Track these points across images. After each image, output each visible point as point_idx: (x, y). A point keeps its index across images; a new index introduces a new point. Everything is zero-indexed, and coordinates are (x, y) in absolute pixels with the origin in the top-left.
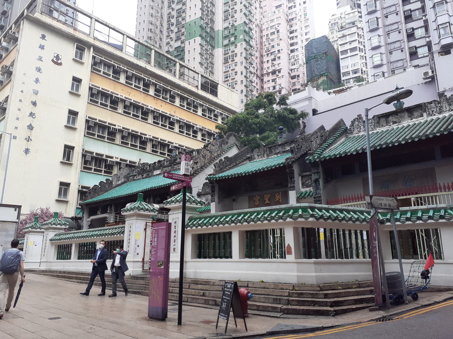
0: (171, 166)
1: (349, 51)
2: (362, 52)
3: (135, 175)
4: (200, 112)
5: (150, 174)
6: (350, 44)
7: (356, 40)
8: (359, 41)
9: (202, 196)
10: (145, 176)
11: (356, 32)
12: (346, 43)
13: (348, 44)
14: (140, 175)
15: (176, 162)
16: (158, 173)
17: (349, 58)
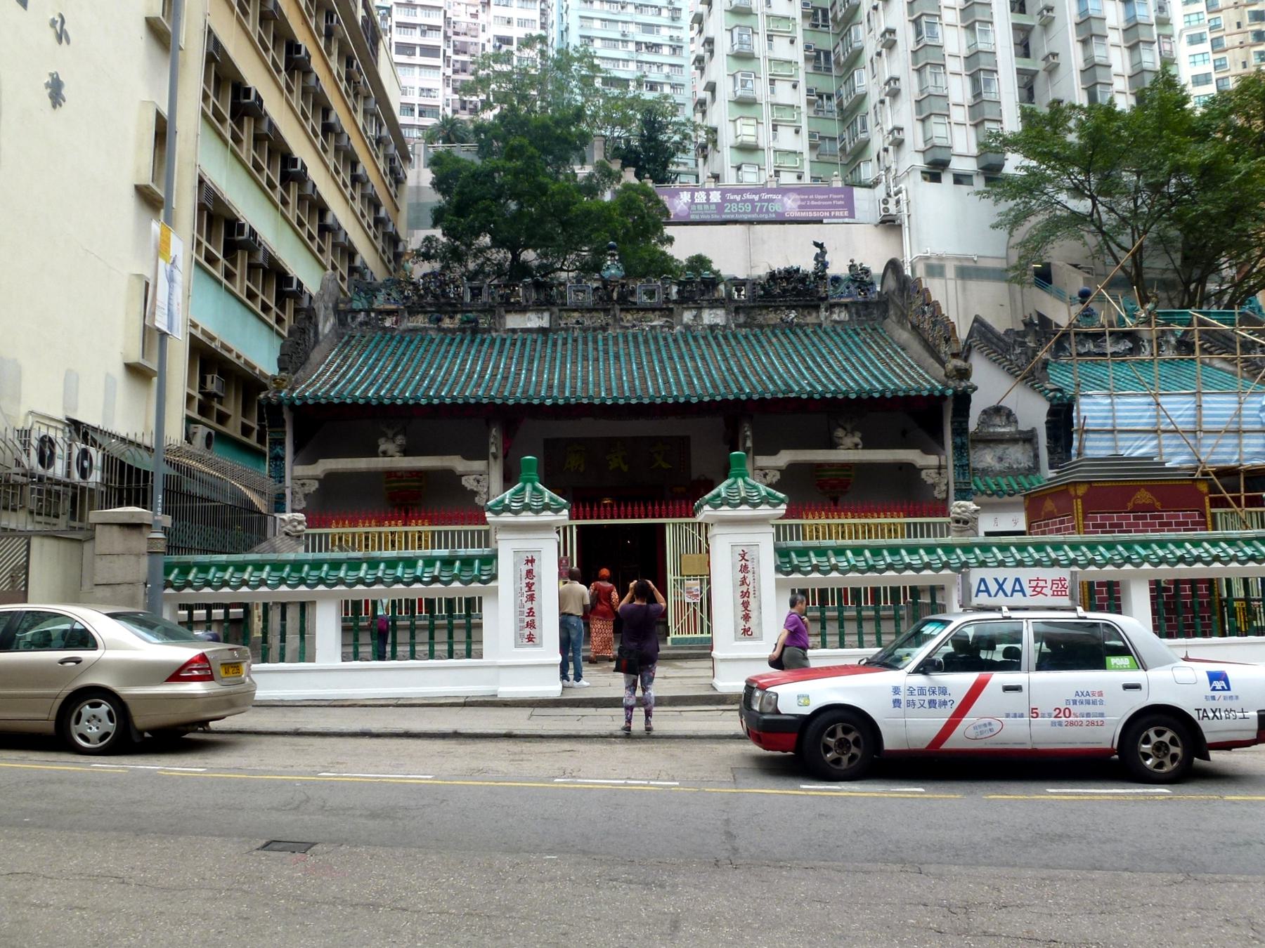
0: (606, 311)
1: (418, 50)
2: (448, 66)
3: (390, 313)
4: (360, 120)
5: (484, 322)
6: (424, 33)
7: (437, 28)
8: (445, 33)
9: (981, 446)
10: (447, 323)
11: (440, 8)
12: (413, 26)
13: (418, 31)
14: (420, 318)
15: (635, 303)
16: (529, 325)
17: (417, 69)
